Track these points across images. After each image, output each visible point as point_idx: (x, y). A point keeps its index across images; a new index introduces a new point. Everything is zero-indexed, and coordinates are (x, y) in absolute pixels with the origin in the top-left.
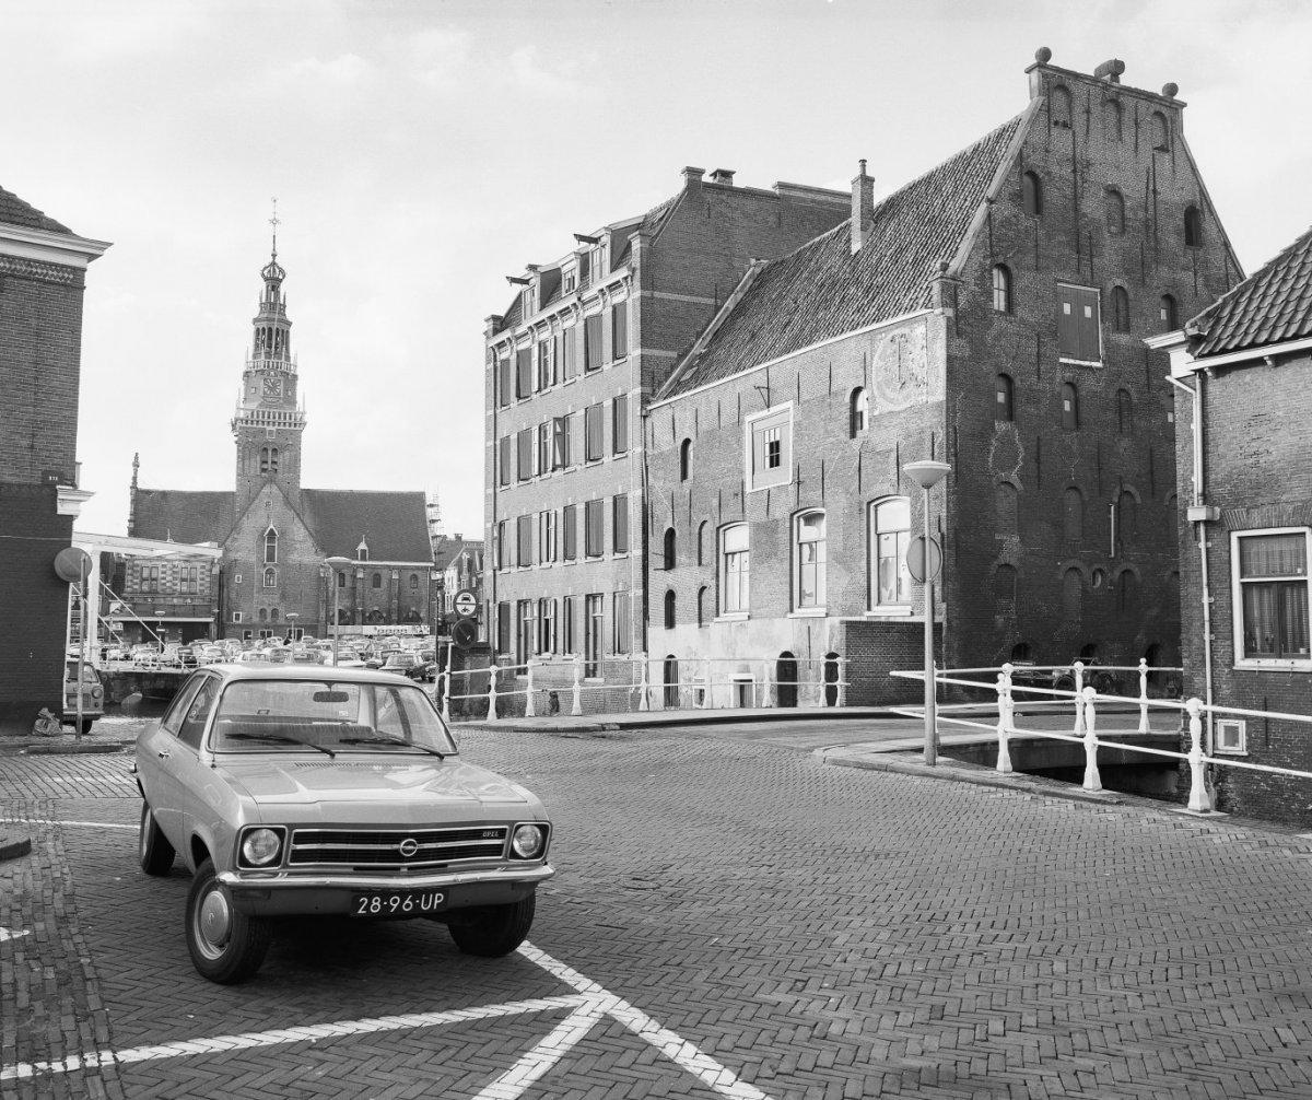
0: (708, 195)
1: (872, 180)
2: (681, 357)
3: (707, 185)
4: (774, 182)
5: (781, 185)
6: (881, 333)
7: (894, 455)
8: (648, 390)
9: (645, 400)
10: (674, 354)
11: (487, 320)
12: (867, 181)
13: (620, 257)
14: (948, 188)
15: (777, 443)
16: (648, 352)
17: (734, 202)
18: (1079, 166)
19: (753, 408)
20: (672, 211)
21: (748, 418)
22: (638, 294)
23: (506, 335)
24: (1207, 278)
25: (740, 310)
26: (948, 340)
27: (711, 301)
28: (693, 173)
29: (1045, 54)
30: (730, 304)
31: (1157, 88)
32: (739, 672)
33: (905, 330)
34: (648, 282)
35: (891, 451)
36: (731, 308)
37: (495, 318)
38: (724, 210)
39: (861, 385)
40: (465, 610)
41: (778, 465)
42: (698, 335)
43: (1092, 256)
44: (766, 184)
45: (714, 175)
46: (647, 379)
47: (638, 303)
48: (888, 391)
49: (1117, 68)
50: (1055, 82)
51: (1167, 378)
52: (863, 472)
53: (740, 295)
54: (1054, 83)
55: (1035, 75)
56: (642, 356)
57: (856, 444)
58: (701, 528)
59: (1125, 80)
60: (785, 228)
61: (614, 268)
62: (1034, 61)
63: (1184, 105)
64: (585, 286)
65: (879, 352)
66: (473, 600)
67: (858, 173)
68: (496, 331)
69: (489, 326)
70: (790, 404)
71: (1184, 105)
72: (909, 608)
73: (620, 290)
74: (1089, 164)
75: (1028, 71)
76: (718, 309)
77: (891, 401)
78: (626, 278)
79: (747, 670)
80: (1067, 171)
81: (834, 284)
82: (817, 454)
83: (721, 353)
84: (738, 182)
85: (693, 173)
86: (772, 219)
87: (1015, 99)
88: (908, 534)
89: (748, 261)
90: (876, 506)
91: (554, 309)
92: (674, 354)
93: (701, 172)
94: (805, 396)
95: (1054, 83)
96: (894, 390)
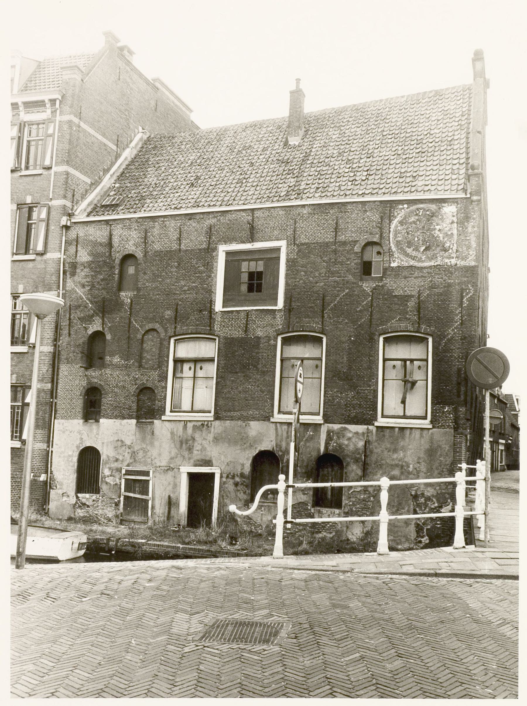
6: (403, 204)
10: (89, 181)
15: (260, 274)
19: (228, 240)
21: (222, 249)
32: (196, 465)
33: (433, 207)
35: (413, 296)
36: (129, 159)
41: (259, 290)
46: (70, 195)
48: (409, 251)
57: (367, 286)
58: (144, 335)
65: (398, 218)
73: (42, 109)
77: (414, 258)
79: (208, 463)
82: (315, 289)
92: (89, 181)
96: (417, 249)
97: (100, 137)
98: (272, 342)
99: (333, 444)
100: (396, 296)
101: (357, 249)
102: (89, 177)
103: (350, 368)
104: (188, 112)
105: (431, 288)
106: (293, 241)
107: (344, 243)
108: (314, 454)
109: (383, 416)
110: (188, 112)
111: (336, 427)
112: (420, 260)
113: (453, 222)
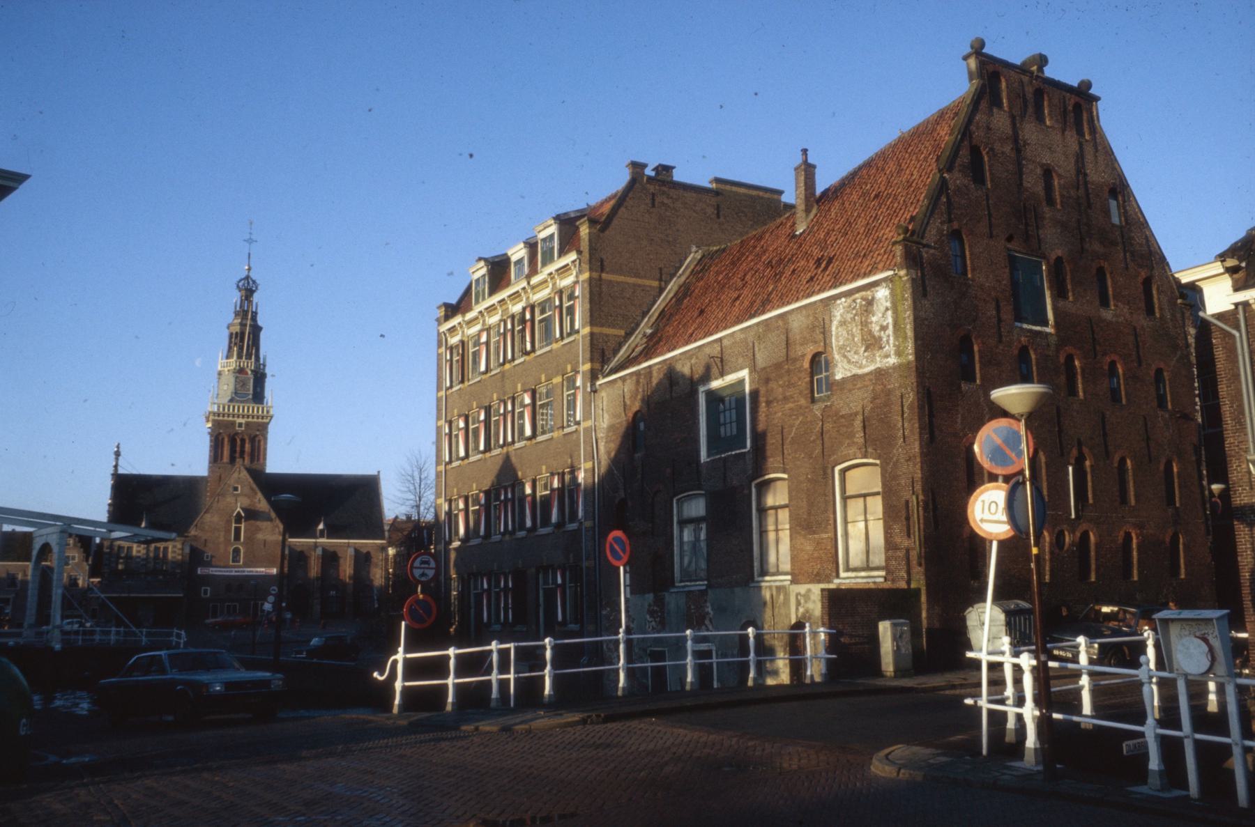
0: (651, 189)
1: (814, 167)
2: (628, 335)
3: (649, 178)
4: (712, 177)
5: (717, 180)
7: (860, 418)
8: (597, 366)
9: (593, 376)
10: (622, 333)
11: (439, 308)
12: (808, 171)
13: (568, 239)
14: (891, 167)
16: (597, 330)
17: (673, 193)
18: (1018, 146)
20: (621, 200)
22: (586, 275)
23: (457, 320)
24: (1133, 254)
25: (684, 292)
26: (914, 302)
27: (655, 284)
28: (637, 167)
29: (982, 44)
30: (672, 286)
31: (1074, 82)
33: (868, 294)
34: (597, 261)
35: (856, 414)
36: (676, 288)
37: (447, 306)
38: (666, 201)
39: (820, 350)
40: (423, 575)
42: (644, 314)
43: (1038, 228)
44: (704, 181)
45: (656, 169)
46: (597, 355)
47: (586, 285)
49: (1042, 60)
50: (990, 68)
51: (1201, 314)
52: (826, 437)
53: (683, 279)
54: (990, 72)
55: (973, 63)
56: (592, 334)
57: (817, 409)
59: (1049, 72)
60: (722, 219)
61: (562, 252)
62: (969, 50)
63: (1097, 99)
64: (534, 271)
66: (433, 564)
67: (799, 159)
68: (447, 318)
69: (442, 313)
70: (744, 373)
71: (1097, 99)
72: (883, 573)
74: (1026, 143)
75: (965, 58)
76: (661, 290)
78: (574, 262)
80: (1008, 149)
81: (781, 261)
83: (670, 329)
84: (678, 176)
85: (637, 167)
86: (710, 211)
87: (954, 85)
88: (879, 499)
89: (689, 248)
90: (844, 471)
91: (504, 294)
93: (645, 166)
94: (761, 362)
95: (990, 72)
97: (631, 280)
98: (746, 492)
99: (801, 610)
100: (842, 417)
101: (806, 365)
102: (621, 328)
103: (809, 514)
104: (776, 197)
105: (874, 398)
106: (753, 370)
107: (795, 360)
108: (786, 622)
109: (848, 569)
110: (776, 197)
111: (802, 589)
112: (860, 367)
113: (887, 309)
